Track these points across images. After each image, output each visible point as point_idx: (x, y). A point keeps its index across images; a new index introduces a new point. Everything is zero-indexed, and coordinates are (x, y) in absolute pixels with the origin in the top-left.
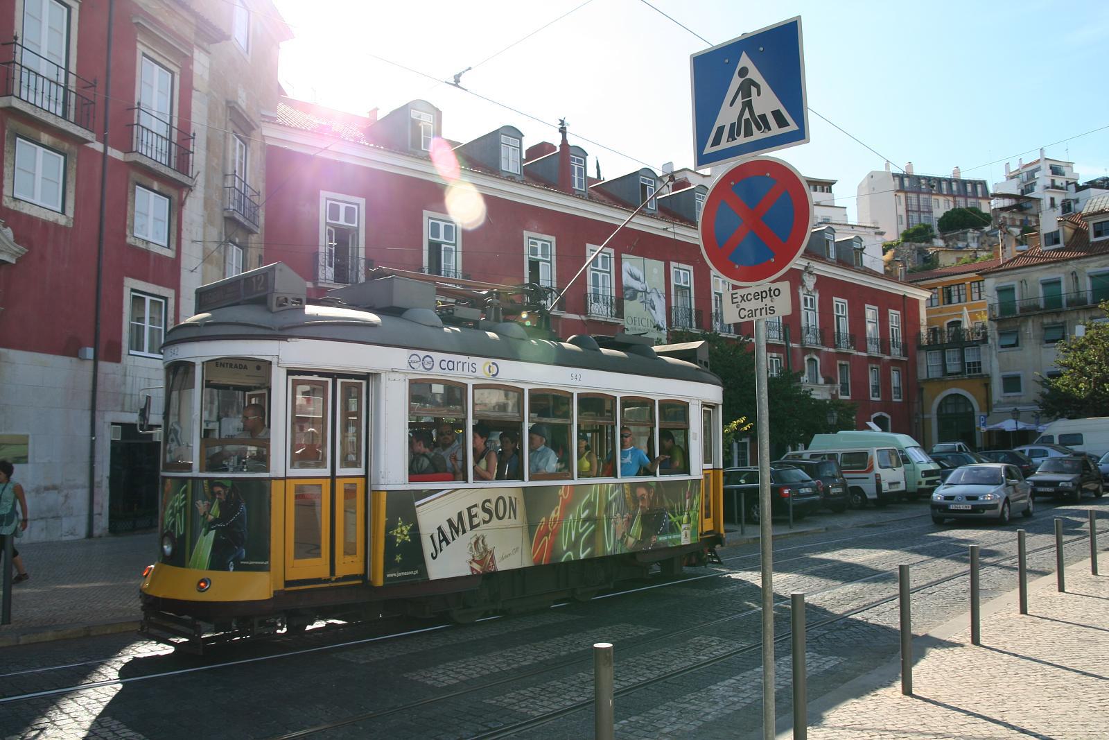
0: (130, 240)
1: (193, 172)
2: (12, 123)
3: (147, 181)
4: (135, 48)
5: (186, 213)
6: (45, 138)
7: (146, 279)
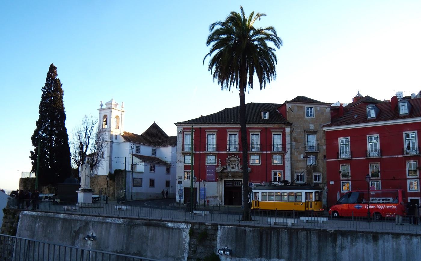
0: (272, 164)
1: (287, 150)
2: (250, 154)
3: (275, 154)
4: (272, 134)
5: (286, 157)
6: (255, 154)
7: (276, 170)
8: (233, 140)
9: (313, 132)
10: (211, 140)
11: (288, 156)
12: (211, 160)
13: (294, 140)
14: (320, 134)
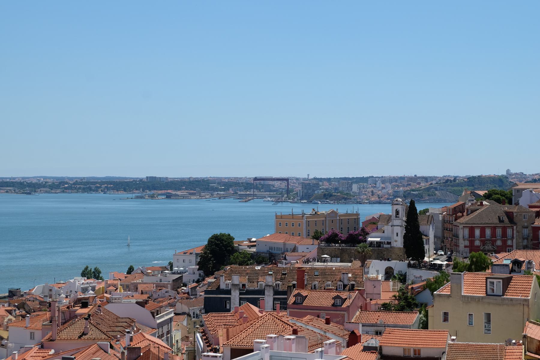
8: (488, 232)
9: (527, 227)
10: (477, 232)
11: (514, 240)
12: (477, 243)
13: (518, 232)
14: (530, 228)
